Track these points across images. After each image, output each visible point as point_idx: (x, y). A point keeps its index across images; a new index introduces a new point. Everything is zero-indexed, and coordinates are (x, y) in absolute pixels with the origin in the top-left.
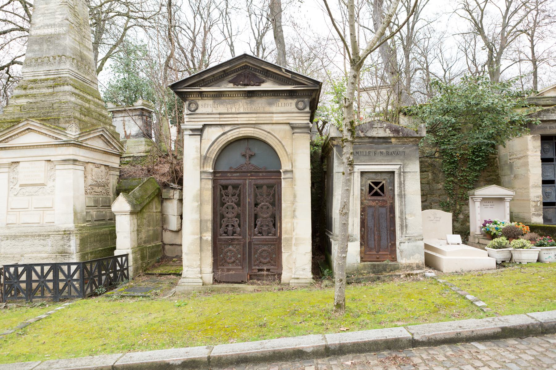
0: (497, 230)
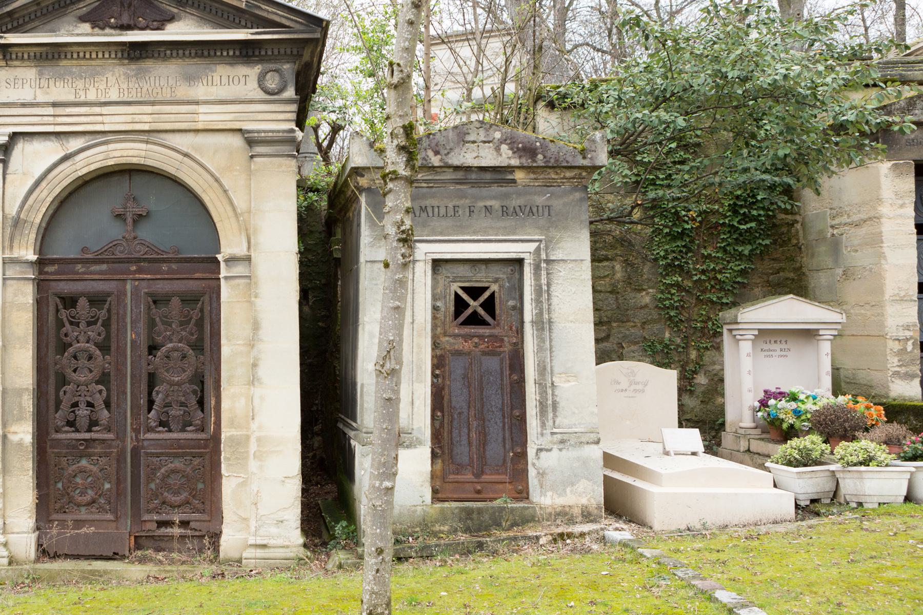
0: (798, 417)
